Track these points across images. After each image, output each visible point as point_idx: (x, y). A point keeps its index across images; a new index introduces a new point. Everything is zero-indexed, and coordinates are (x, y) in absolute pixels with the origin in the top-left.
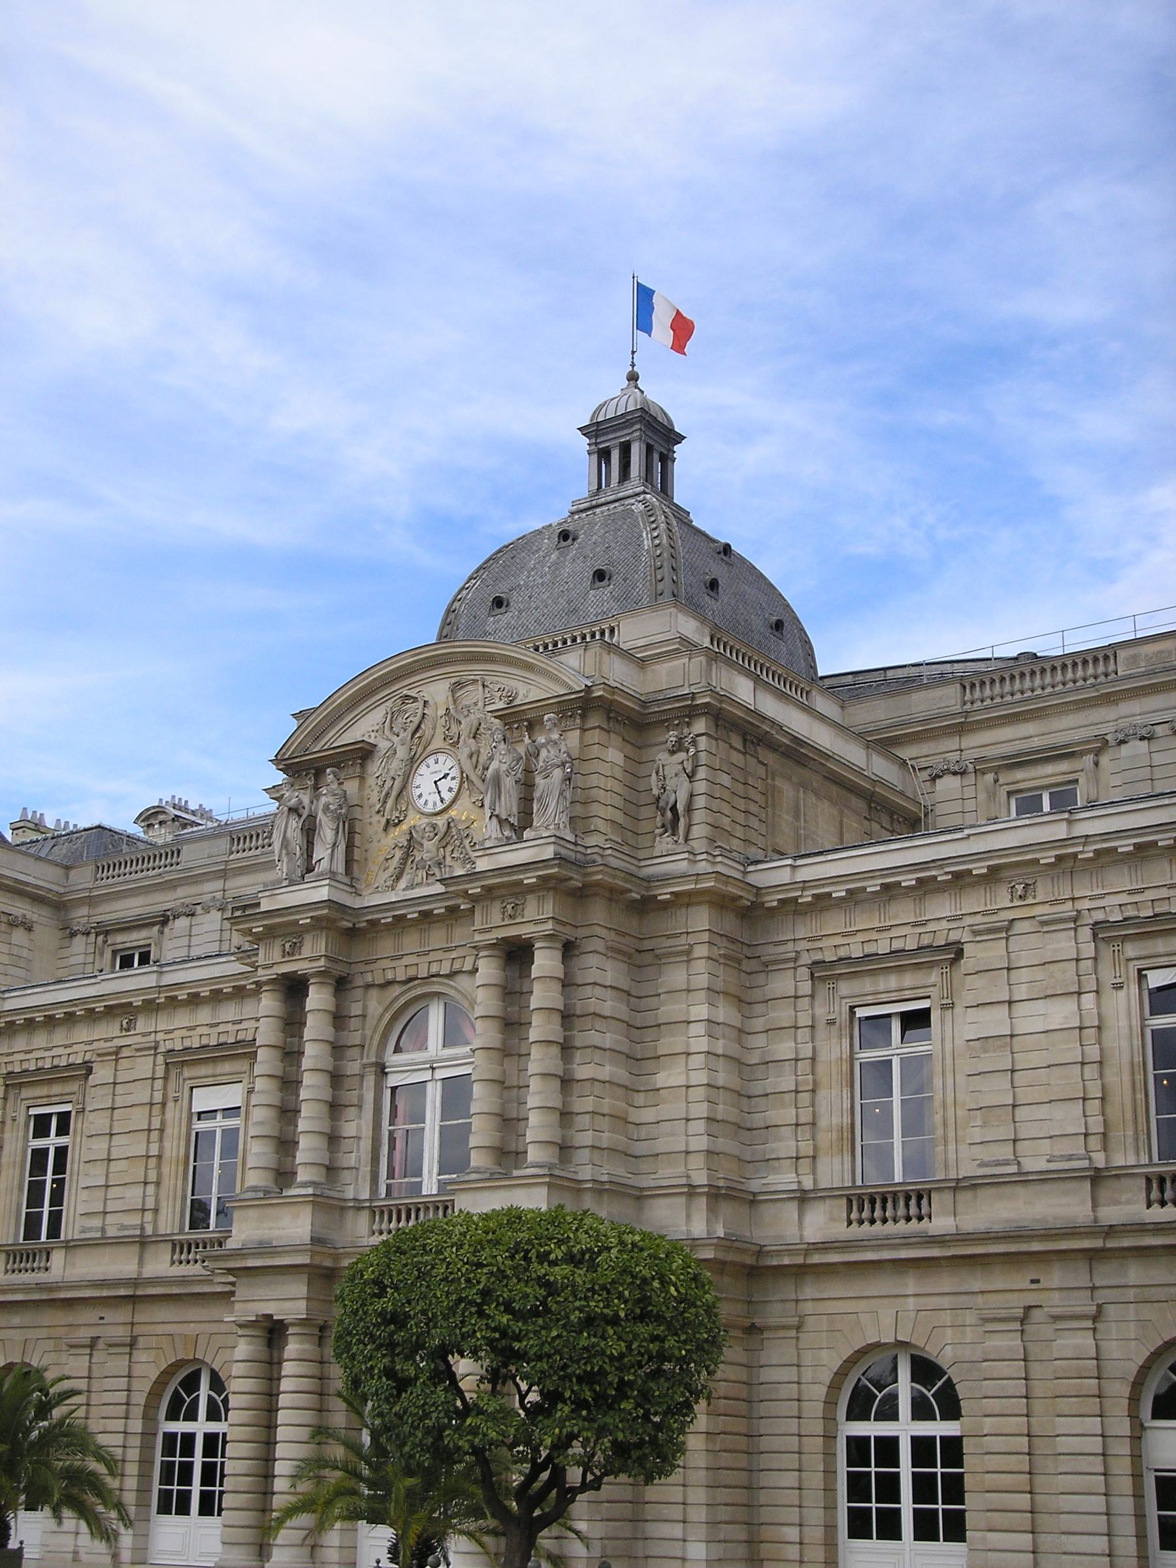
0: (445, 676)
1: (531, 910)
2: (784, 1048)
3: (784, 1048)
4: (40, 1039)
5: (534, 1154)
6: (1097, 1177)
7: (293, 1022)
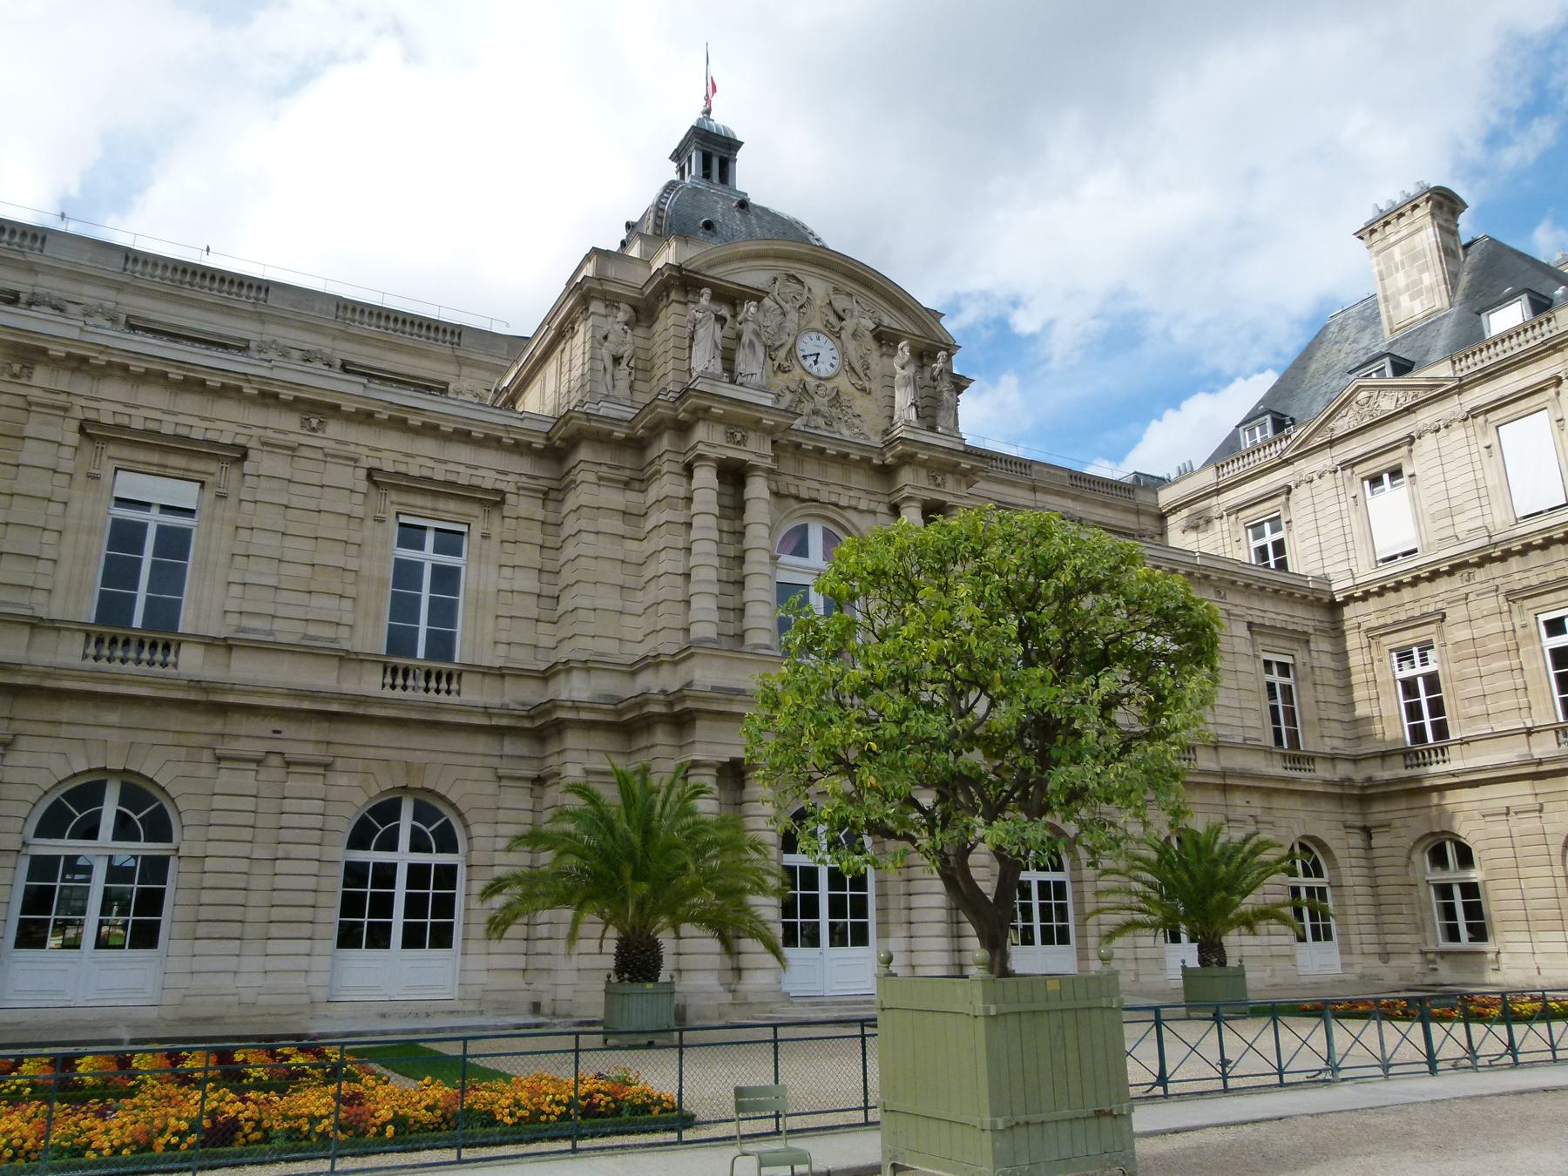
0: (823, 278)
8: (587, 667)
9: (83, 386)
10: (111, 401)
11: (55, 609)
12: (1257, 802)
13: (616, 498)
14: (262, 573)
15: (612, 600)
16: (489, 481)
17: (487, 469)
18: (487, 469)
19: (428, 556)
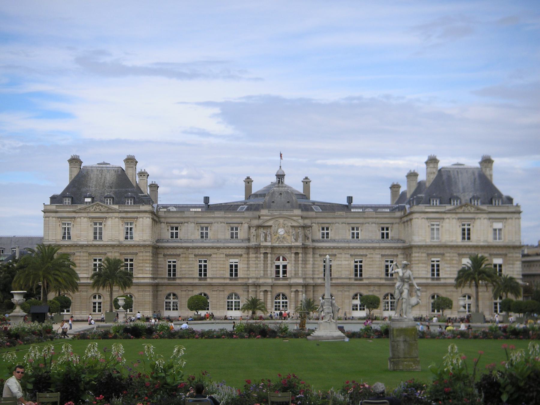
1: (299, 249)
2: (316, 263)
3: (316, 263)
4: (201, 250)
5: (300, 275)
6: (350, 278)
7: (266, 257)
8: (251, 278)
10: (197, 252)
11: (195, 276)
13: (254, 255)
14: (214, 269)
15: (254, 269)
16: (240, 253)
17: (240, 252)
18: (240, 252)
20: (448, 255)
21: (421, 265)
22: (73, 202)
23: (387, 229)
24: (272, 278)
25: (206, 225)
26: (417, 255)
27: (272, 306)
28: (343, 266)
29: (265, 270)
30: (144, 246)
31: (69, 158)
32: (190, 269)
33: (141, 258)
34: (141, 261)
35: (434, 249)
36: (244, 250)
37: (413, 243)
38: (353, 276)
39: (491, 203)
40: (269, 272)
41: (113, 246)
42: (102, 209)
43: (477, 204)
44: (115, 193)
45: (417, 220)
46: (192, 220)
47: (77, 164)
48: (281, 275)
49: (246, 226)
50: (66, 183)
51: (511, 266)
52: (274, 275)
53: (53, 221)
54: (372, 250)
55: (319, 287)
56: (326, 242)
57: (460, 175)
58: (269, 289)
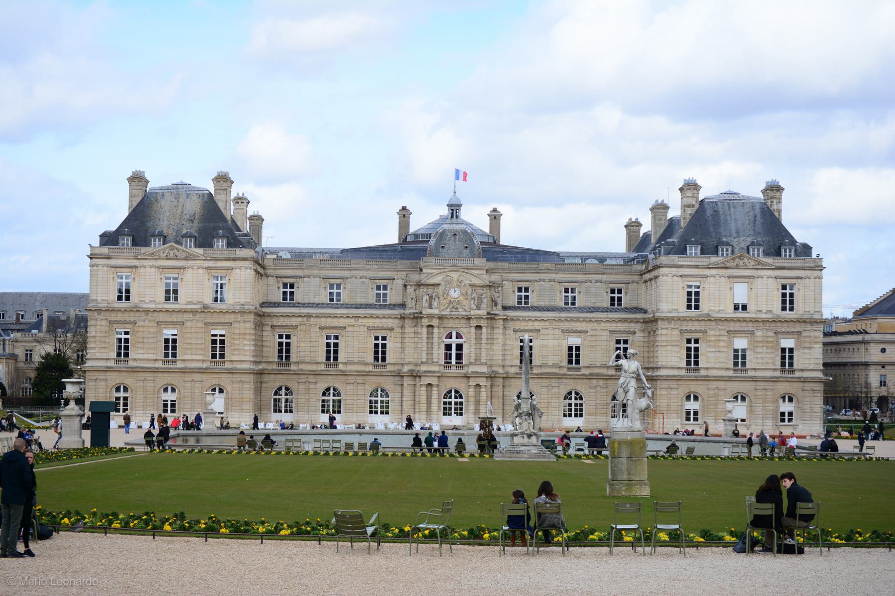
2: (508, 342)
3: (508, 342)
4: (329, 320)
5: (483, 361)
6: (560, 367)
7: (430, 334)
9: (318, 320)
10: (323, 322)
11: (319, 360)
12: (601, 382)
13: (412, 330)
17: (389, 323)
18: (389, 323)
19: (380, 342)
20: (711, 333)
21: (669, 348)
22: (135, 243)
23: (620, 291)
24: (440, 365)
25: (338, 281)
26: (664, 332)
27: (439, 409)
28: (550, 347)
29: (430, 353)
30: (242, 313)
31: (130, 174)
32: (313, 349)
33: (237, 331)
34: (238, 337)
35: (690, 323)
36: (397, 321)
37: (657, 314)
38: (565, 363)
39: (778, 253)
40: (435, 355)
41: (194, 312)
42: (177, 253)
43: (758, 255)
44: (200, 231)
45: (665, 277)
46: (315, 272)
47: (140, 183)
48: (454, 360)
49: (400, 283)
50: (124, 213)
51: (807, 351)
52: (442, 361)
53: (104, 272)
54: (595, 324)
55: (513, 380)
56: (524, 309)
57: (732, 210)
58: (434, 381)
